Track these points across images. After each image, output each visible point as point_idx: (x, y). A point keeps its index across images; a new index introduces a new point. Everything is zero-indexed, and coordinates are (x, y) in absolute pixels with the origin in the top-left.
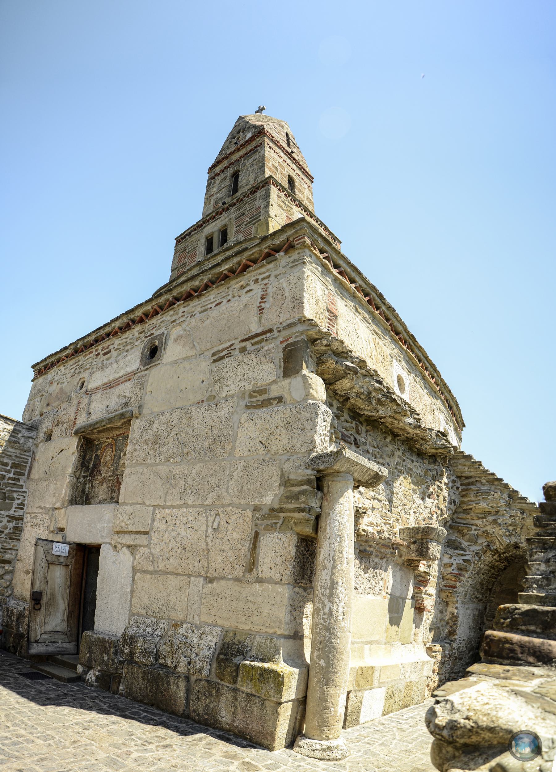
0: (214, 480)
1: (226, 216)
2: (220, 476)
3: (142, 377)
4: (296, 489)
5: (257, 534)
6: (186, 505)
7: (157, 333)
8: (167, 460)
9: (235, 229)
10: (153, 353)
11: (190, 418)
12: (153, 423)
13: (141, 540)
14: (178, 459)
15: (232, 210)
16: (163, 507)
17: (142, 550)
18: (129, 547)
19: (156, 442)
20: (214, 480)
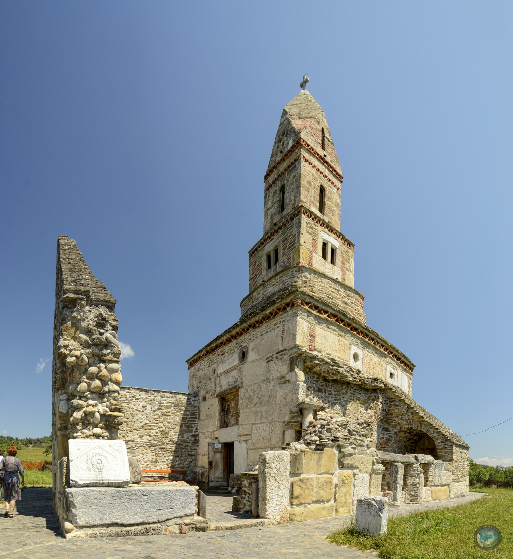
0: (270, 413)
1: (277, 237)
2: (272, 411)
3: (240, 368)
4: (294, 415)
5: (284, 431)
6: (262, 423)
7: (244, 345)
8: (255, 405)
9: (282, 251)
10: (243, 356)
11: (261, 388)
12: (248, 390)
13: (248, 437)
14: (258, 405)
15: (280, 232)
16: (255, 424)
17: (249, 441)
18: (245, 441)
19: (250, 398)
20: (270, 413)
